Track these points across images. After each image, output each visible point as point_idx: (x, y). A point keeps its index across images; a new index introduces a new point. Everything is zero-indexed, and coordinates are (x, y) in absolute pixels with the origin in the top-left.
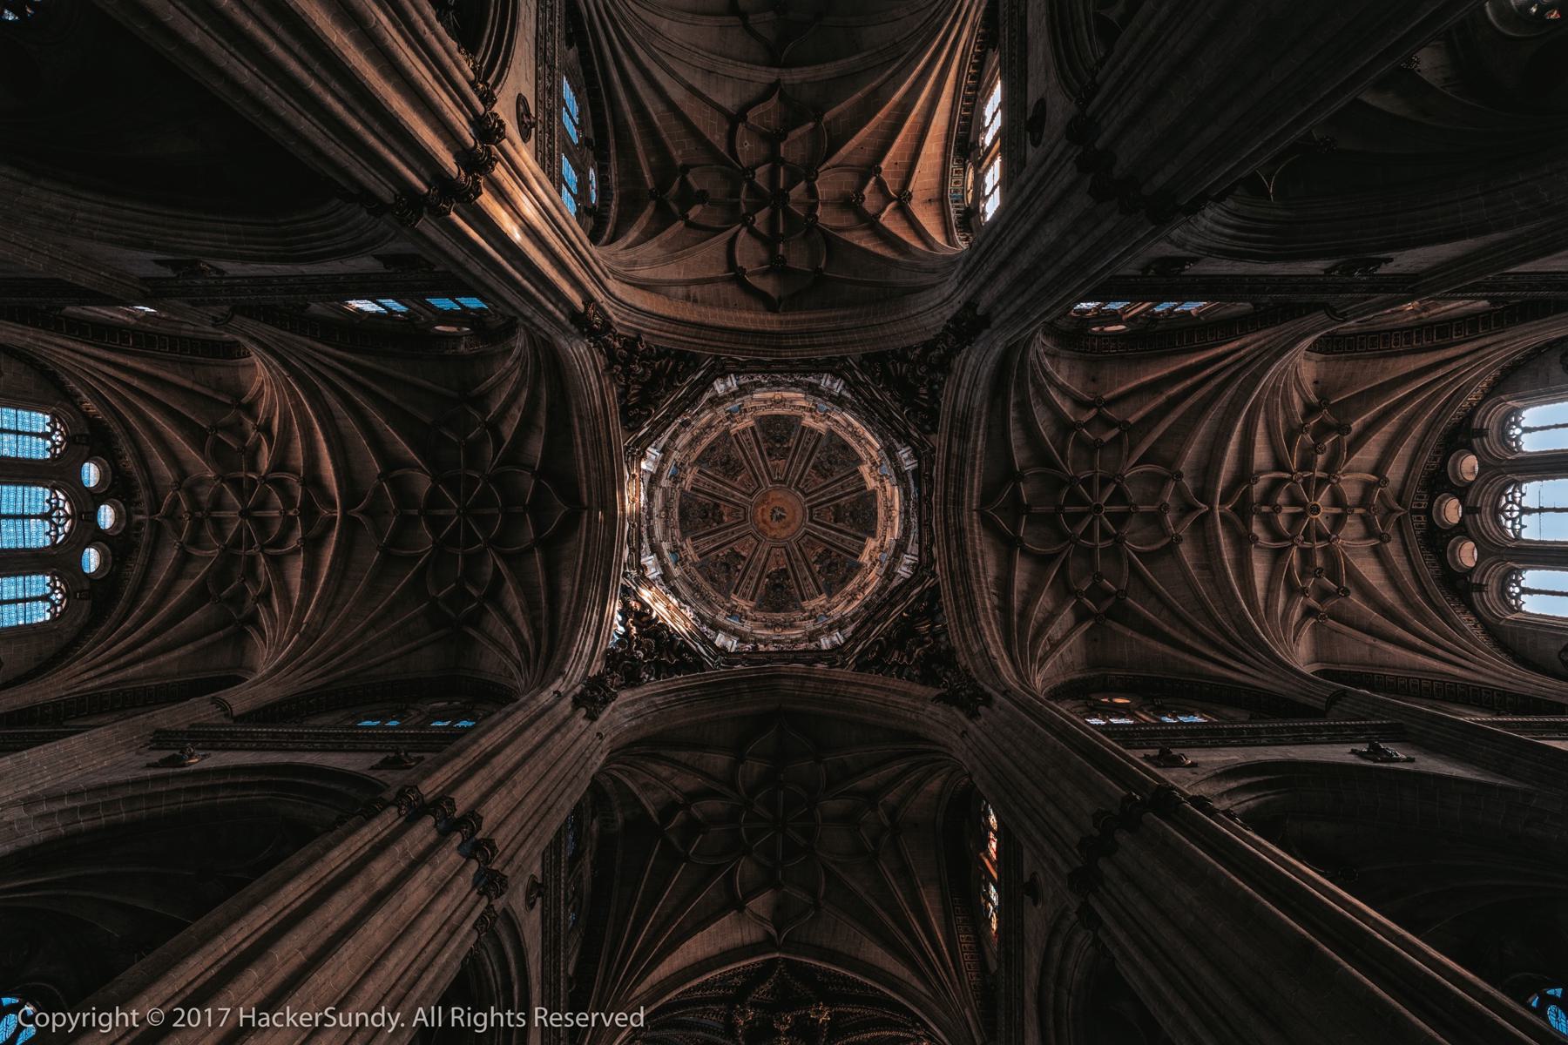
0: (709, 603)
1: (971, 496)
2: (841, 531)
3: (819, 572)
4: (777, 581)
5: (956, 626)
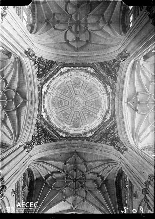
3: (87, 118)
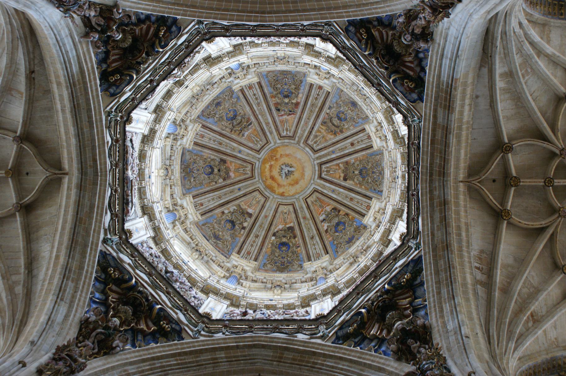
0: (207, 262)
1: (457, 167)
3: (326, 231)
4: (284, 240)
5: (434, 300)
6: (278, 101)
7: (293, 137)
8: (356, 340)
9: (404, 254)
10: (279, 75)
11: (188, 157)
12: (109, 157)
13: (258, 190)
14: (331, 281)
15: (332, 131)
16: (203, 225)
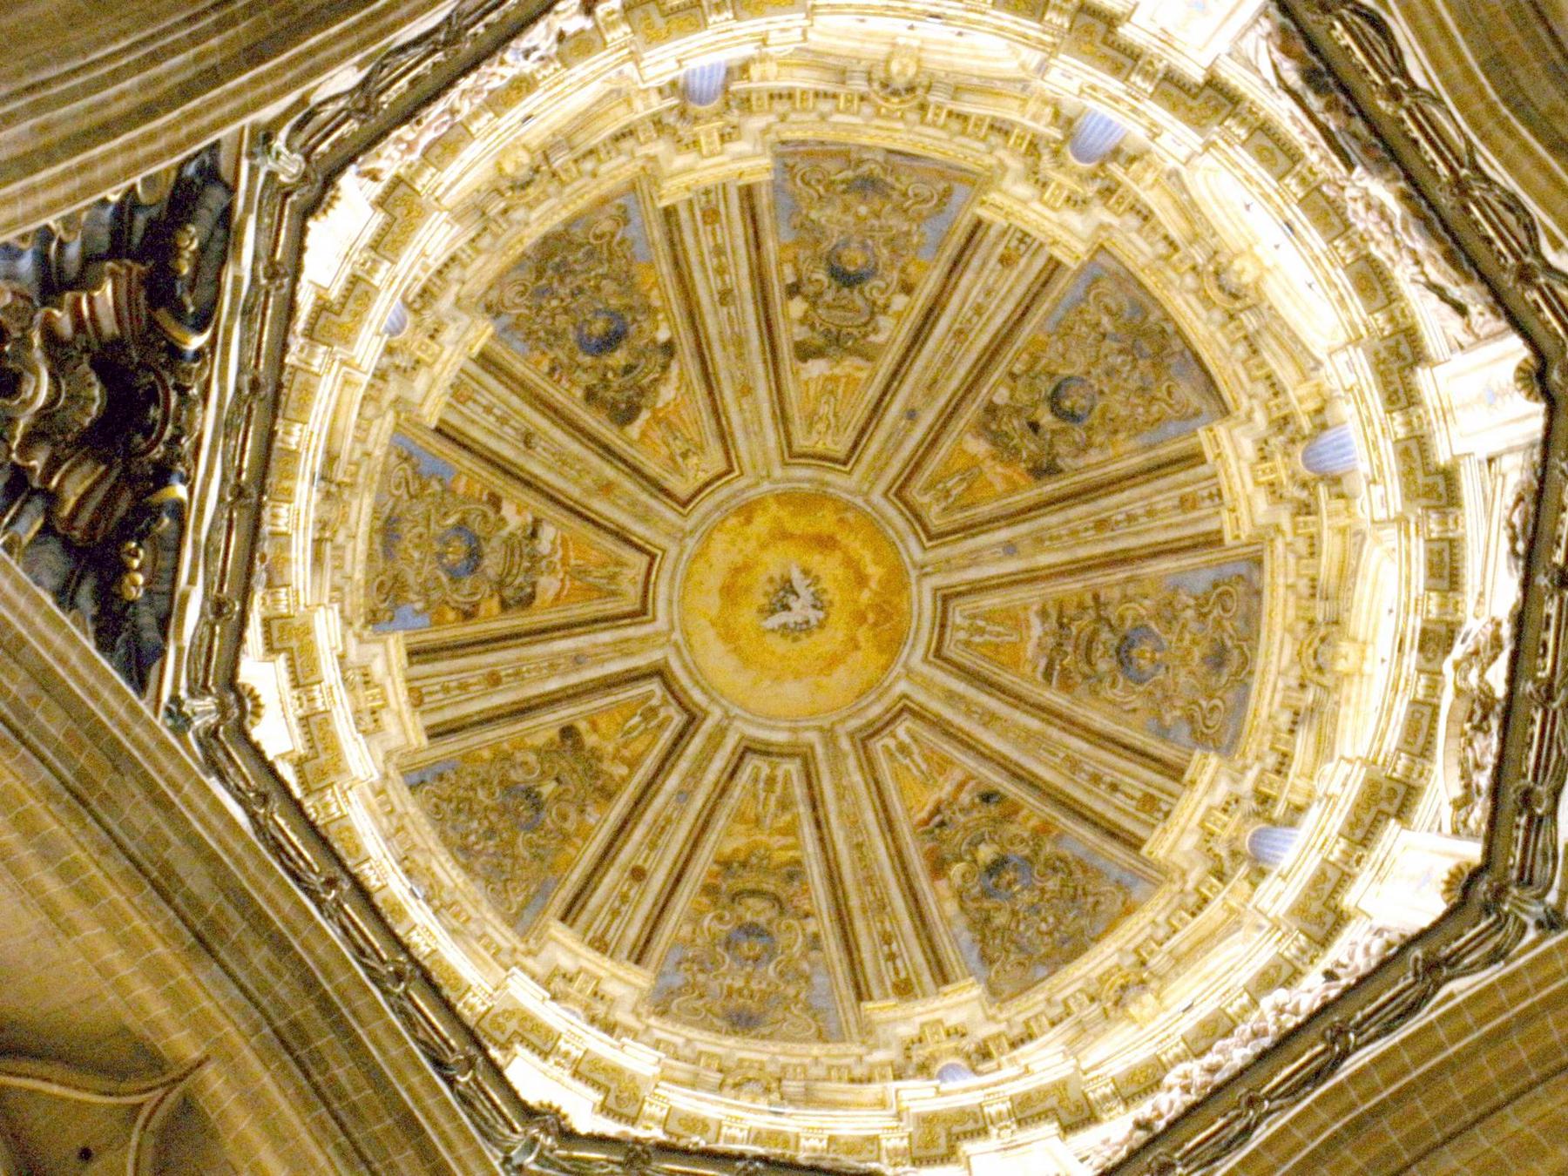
0: (842, 75)
1: (255, 1102)
2: (521, 711)
3: (495, 501)
4: (619, 358)
6: (1013, 829)
7: (864, 741)
8: (140, 221)
9: (202, 650)
10: (1084, 922)
11: (1187, 392)
12: (1513, 196)
13: (845, 463)
14: (367, 348)
15: (744, 865)
16: (947, 193)
